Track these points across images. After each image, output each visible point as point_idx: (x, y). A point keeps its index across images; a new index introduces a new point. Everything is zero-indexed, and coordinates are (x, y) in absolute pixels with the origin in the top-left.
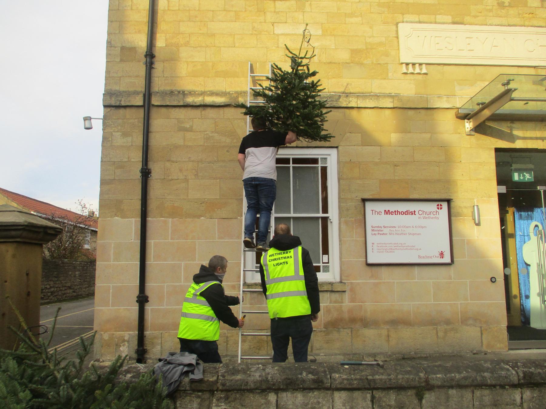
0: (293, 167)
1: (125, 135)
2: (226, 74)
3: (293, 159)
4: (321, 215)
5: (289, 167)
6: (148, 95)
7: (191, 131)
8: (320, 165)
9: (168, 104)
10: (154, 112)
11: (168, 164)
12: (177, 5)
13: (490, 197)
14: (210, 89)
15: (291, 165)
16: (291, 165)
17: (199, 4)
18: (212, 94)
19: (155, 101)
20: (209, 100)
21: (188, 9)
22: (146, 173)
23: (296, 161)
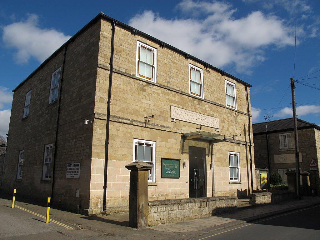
1: (100, 129)
2: (130, 113)
8: (151, 146)
10: (111, 123)
11: (113, 141)
15: (144, 145)
16: (144, 145)
18: (126, 119)
19: (111, 119)
20: (125, 121)
22: (107, 144)
23: (146, 144)
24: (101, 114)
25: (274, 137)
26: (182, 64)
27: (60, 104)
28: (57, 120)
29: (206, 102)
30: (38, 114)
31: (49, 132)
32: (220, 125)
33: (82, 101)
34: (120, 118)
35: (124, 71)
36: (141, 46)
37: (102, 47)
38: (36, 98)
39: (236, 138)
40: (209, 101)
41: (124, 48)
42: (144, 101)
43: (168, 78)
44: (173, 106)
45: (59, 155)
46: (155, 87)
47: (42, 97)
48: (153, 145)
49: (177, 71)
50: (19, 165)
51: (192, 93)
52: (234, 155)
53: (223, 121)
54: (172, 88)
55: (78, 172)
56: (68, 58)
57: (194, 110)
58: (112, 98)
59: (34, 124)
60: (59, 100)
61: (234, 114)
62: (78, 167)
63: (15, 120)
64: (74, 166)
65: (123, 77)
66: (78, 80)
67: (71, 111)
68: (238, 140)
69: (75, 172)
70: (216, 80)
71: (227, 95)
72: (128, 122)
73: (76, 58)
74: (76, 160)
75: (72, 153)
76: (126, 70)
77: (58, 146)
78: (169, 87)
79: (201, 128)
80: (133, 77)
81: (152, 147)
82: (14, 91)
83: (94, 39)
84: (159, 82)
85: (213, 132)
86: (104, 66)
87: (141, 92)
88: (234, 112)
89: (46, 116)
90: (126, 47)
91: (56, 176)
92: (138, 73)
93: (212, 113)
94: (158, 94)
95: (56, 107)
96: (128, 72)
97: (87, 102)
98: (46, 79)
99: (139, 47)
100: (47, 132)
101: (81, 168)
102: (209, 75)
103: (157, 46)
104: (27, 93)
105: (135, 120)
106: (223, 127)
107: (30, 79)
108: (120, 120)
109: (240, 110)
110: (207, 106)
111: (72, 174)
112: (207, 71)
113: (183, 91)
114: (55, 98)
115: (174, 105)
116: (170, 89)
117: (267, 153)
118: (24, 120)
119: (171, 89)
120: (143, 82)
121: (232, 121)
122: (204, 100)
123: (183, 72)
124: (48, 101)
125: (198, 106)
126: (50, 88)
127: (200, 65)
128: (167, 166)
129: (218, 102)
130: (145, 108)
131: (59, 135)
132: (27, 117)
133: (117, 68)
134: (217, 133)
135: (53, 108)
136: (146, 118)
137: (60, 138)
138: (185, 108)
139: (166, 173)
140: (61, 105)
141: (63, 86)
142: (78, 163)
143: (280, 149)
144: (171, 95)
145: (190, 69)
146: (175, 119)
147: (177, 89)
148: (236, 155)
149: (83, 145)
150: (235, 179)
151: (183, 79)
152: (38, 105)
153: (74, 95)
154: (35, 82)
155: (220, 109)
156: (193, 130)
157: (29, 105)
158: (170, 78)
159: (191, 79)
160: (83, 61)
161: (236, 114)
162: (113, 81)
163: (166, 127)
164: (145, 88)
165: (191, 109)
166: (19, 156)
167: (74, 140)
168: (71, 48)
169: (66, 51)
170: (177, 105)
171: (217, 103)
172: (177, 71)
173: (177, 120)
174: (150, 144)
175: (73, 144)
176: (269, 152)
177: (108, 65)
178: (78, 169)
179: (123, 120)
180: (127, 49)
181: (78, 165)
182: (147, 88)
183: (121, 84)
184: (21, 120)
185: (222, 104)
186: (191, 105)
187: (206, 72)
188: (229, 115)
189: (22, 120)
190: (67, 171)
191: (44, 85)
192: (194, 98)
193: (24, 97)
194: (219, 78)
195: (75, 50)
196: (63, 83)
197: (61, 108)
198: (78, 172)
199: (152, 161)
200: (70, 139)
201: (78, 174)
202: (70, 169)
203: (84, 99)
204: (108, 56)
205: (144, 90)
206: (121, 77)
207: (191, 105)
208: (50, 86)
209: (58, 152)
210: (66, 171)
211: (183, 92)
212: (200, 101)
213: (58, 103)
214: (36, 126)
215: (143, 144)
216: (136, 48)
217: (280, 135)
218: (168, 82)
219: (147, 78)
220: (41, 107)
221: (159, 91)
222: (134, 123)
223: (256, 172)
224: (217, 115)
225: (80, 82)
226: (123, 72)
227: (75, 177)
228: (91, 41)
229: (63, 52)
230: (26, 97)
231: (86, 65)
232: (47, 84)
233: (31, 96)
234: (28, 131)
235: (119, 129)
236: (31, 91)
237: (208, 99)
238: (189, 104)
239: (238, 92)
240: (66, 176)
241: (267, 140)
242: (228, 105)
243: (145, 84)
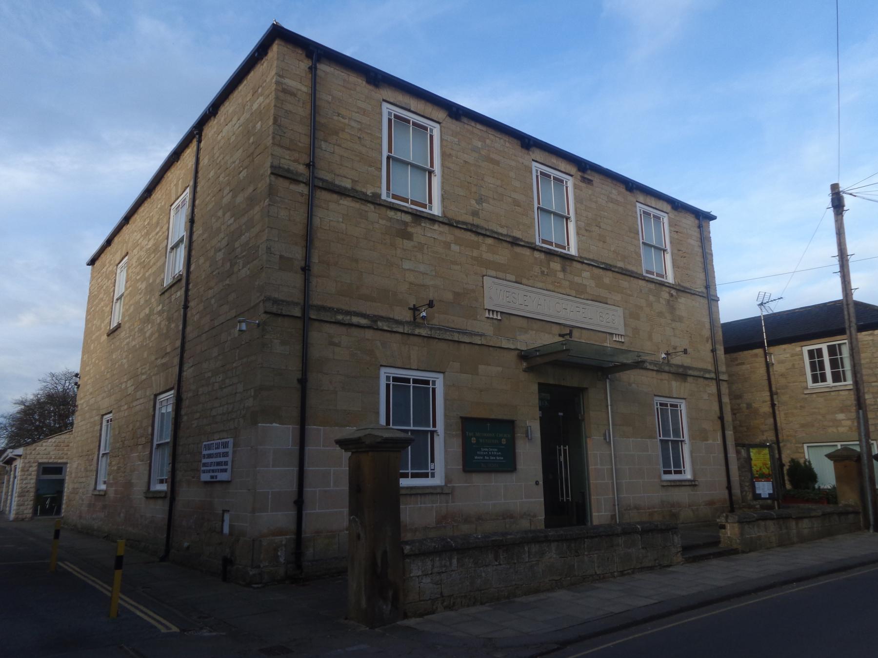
0: (413, 386)
3: (413, 379)
4: (431, 428)
5: (410, 386)
6: (306, 307)
7: (339, 346)
9: (322, 318)
12: (328, 225)
14: (354, 310)
17: (346, 229)
20: (355, 320)
21: (337, 231)
23: (416, 381)
24: (283, 301)
25: (788, 355)
26: (513, 164)
27: (188, 284)
28: (181, 327)
29: (583, 263)
30: (141, 317)
31: (164, 361)
32: (625, 325)
33: (236, 269)
34: (339, 311)
35: (347, 184)
36: (396, 116)
37: (283, 119)
38: (138, 274)
39: (677, 360)
40: (593, 260)
41: (346, 121)
42: (407, 265)
43: (473, 202)
44: (489, 276)
45: (185, 418)
46: (436, 227)
47: (150, 271)
48: (437, 383)
49: (499, 182)
50: (102, 452)
51: (544, 241)
52: (672, 405)
53: (632, 315)
54: (486, 230)
55: (227, 465)
56: (204, 161)
57: (551, 287)
58: (315, 259)
59: (134, 343)
60: (185, 275)
61: (665, 295)
62: (226, 450)
63: (94, 337)
64: (217, 448)
65: (346, 202)
66: (228, 214)
67: (213, 301)
68: (682, 366)
69: (219, 464)
70: (611, 205)
71: (643, 243)
72: (364, 322)
73: (222, 156)
74: (223, 431)
75: (214, 413)
76: (353, 181)
77: (184, 396)
78: (477, 226)
79: (570, 334)
80: (375, 201)
81: (434, 390)
82: (92, 262)
83: (261, 99)
84: (450, 215)
85: (605, 344)
86: (288, 171)
87: (399, 241)
88: (667, 289)
89: (159, 320)
90: (350, 119)
91: (179, 475)
92: (388, 189)
93: (603, 293)
94: (447, 245)
95: (180, 294)
96: (358, 188)
97: (248, 272)
98: (158, 223)
99: (390, 120)
100: (159, 362)
101: (234, 452)
102: (590, 192)
103: (441, 115)
104: (117, 265)
105: (382, 317)
106: (636, 331)
107: (125, 228)
108: (340, 317)
109: (682, 284)
110: (586, 274)
111: (213, 471)
112: (584, 180)
113: (517, 234)
114: (177, 272)
115: (493, 273)
116: (479, 231)
117: (768, 398)
118: (112, 333)
119: (483, 232)
120: (403, 214)
121: (660, 314)
122: (579, 259)
123: (517, 184)
124: (163, 280)
125: (561, 275)
126: (167, 246)
127: (563, 165)
129: (620, 264)
130: (411, 283)
131: (185, 368)
132: (119, 326)
133: (328, 177)
134: (618, 346)
135: (173, 297)
136: (415, 309)
137: (188, 373)
138: (524, 281)
139: (476, 458)
140: (191, 286)
141: (195, 237)
142: (228, 438)
143: (807, 388)
144: (484, 248)
145: (537, 177)
146: (497, 312)
147: (500, 230)
148: (676, 406)
149: (240, 388)
150: (676, 472)
151: (516, 203)
152: (140, 294)
153: (220, 256)
154: (135, 234)
155: (624, 282)
156: (547, 339)
157: (122, 295)
158: (480, 200)
159: (539, 203)
160: (237, 163)
161: (672, 295)
162: (320, 215)
163: (472, 334)
164: (410, 229)
165: (540, 285)
166: (101, 430)
167: (220, 378)
168: (210, 131)
169: (200, 141)
170: (501, 275)
171: (616, 267)
172: (499, 182)
173: (502, 313)
175: (216, 386)
176: (775, 397)
177: (301, 169)
178: (225, 455)
179: (348, 318)
180: (353, 124)
181: (225, 445)
182: (416, 230)
183: (341, 220)
184: (105, 337)
185: (633, 269)
186: (542, 272)
187: (583, 185)
188: (652, 298)
189: (108, 335)
190: (204, 461)
191: (154, 239)
192: (549, 253)
193: (112, 277)
194: (620, 199)
195: (220, 137)
196: (194, 229)
197: (190, 293)
198: (226, 463)
200: (210, 374)
201: (225, 470)
202: (210, 456)
203: (241, 265)
204: (300, 144)
205: (408, 236)
206: (341, 202)
207: (542, 272)
208: (167, 238)
209: (183, 412)
210: (201, 461)
211: (518, 239)
212: (568, 263)
213: (184, 281)
214: (137, 346)
215: (407, 380)
216: (381, 122)
217: (806, 349)
219: (413, 202)
220: (148, 297)
221: (449, 238)
222: (380, 324)
223: (738, 452)
224: (618, 297)
225: (233, 219)
226: (346, 188)
227: (222, 476)
228: (255, 106)
229: (194, 145)
230: (116, 274)
231: (244, 174)
232: (160, 237)
233: (127, 271)
234: (120, 362)
235: (336, 340)
236: (127, 258)
237: (591, 257)
238: (537, 269)
239: (675, 236)
240: (199, 477)
241: (768, 366)
242: (648, 272)
243: (408, 218)
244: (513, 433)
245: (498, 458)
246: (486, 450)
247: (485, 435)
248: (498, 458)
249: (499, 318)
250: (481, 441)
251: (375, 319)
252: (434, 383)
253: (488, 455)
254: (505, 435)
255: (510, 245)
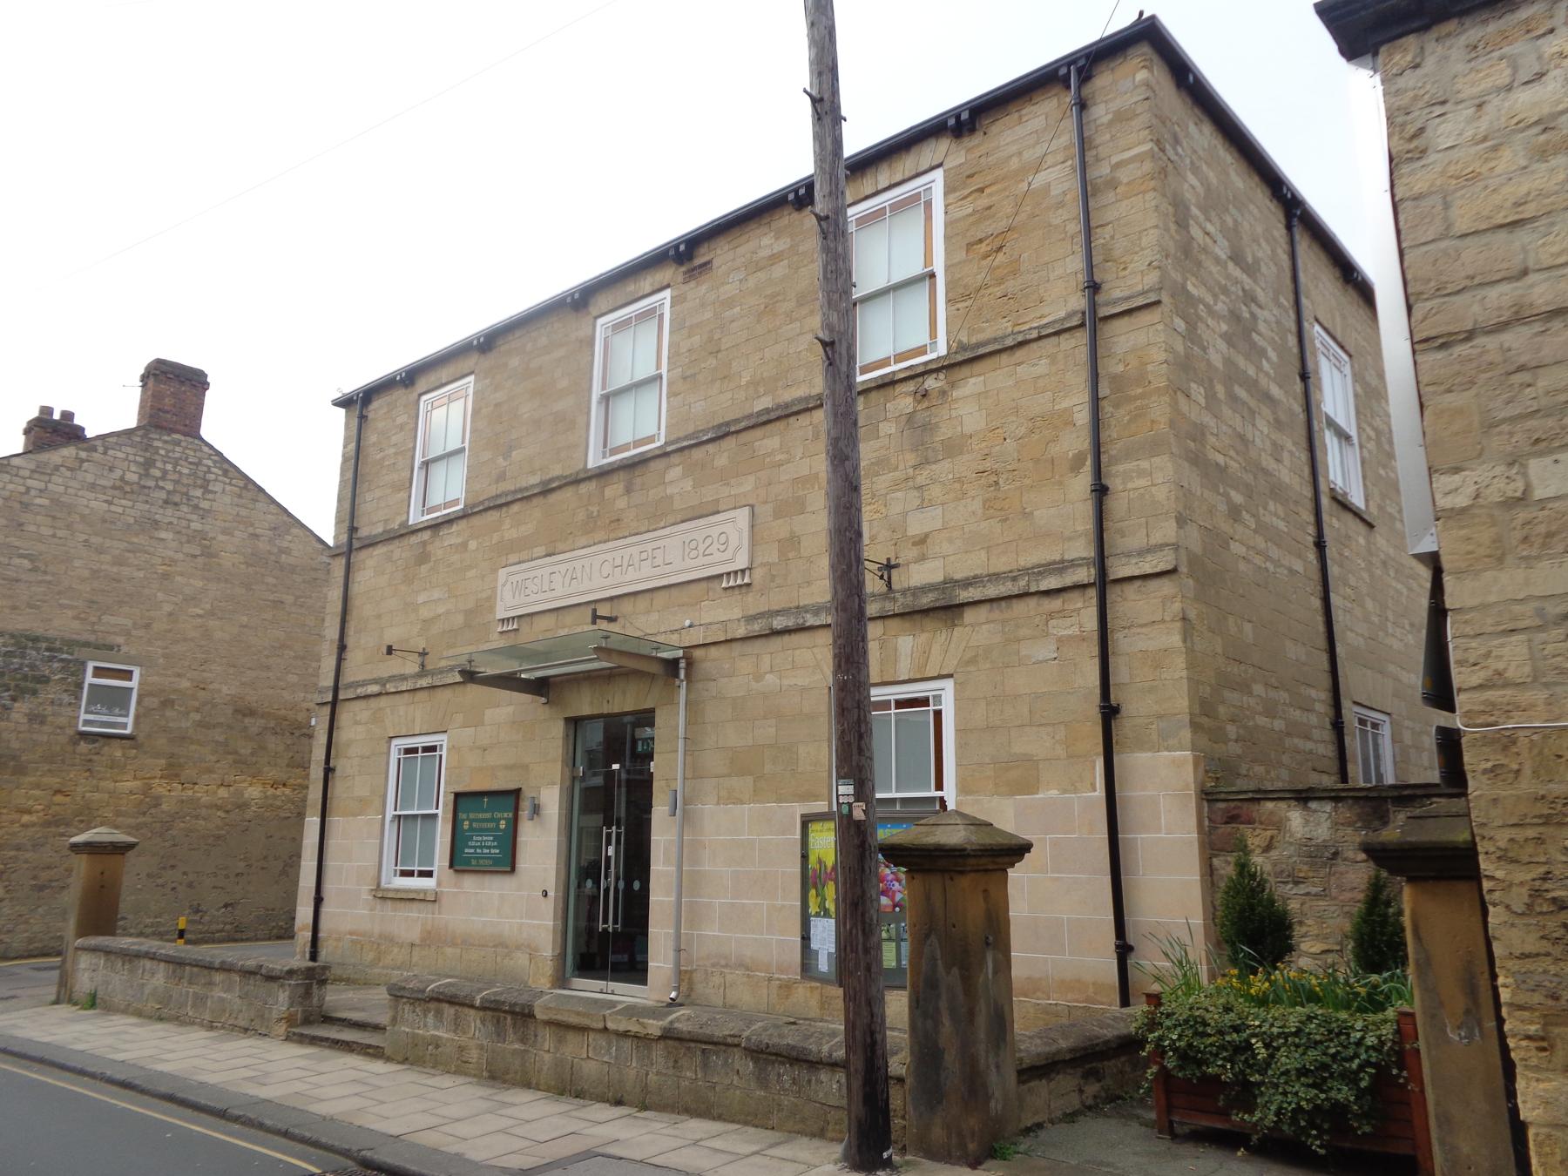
13: (554, 784)
81: (441, 756)
128: (471, 822)
139: (466, 851)
174: (436, 746)
199: (437, 808)
206: (375, 553)
218: (501, 477)
244: (516, 810)
245: (492, 851)
246: (480, 838)
247: (480, 816)
248: (492, 851)
249: (515, 627)
250: (474, 825)
251: (381, 682)
252: (441, 745)
253: (481, 847)
254: (505, 815)
255: (541, 498)
